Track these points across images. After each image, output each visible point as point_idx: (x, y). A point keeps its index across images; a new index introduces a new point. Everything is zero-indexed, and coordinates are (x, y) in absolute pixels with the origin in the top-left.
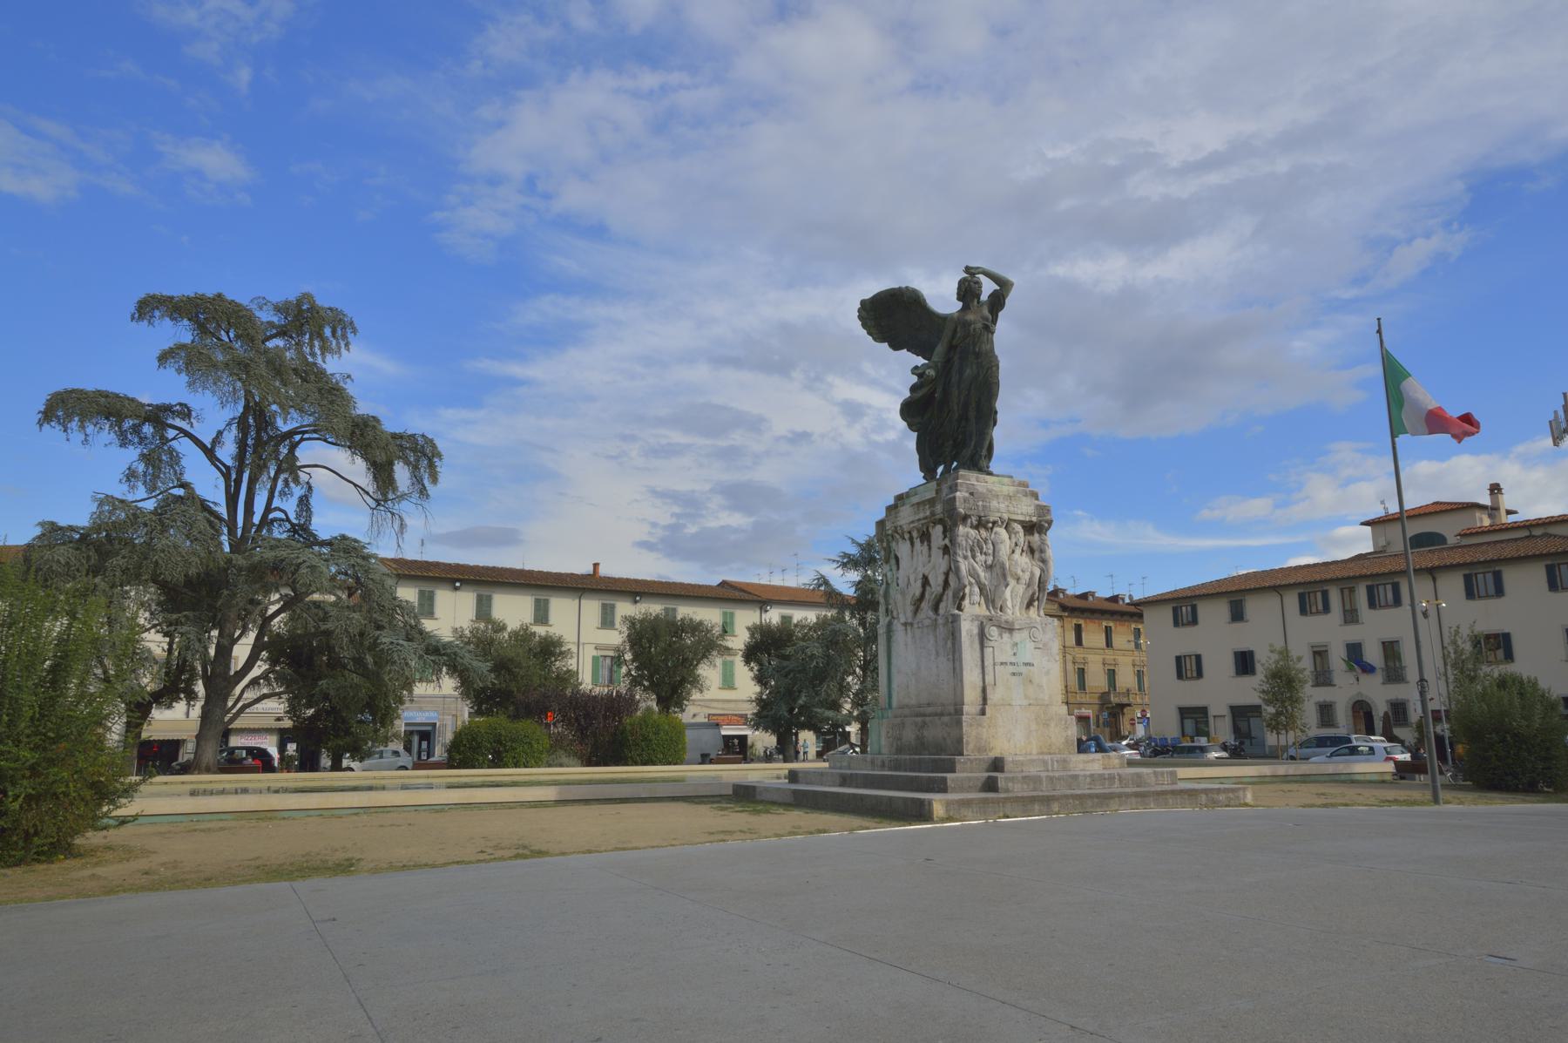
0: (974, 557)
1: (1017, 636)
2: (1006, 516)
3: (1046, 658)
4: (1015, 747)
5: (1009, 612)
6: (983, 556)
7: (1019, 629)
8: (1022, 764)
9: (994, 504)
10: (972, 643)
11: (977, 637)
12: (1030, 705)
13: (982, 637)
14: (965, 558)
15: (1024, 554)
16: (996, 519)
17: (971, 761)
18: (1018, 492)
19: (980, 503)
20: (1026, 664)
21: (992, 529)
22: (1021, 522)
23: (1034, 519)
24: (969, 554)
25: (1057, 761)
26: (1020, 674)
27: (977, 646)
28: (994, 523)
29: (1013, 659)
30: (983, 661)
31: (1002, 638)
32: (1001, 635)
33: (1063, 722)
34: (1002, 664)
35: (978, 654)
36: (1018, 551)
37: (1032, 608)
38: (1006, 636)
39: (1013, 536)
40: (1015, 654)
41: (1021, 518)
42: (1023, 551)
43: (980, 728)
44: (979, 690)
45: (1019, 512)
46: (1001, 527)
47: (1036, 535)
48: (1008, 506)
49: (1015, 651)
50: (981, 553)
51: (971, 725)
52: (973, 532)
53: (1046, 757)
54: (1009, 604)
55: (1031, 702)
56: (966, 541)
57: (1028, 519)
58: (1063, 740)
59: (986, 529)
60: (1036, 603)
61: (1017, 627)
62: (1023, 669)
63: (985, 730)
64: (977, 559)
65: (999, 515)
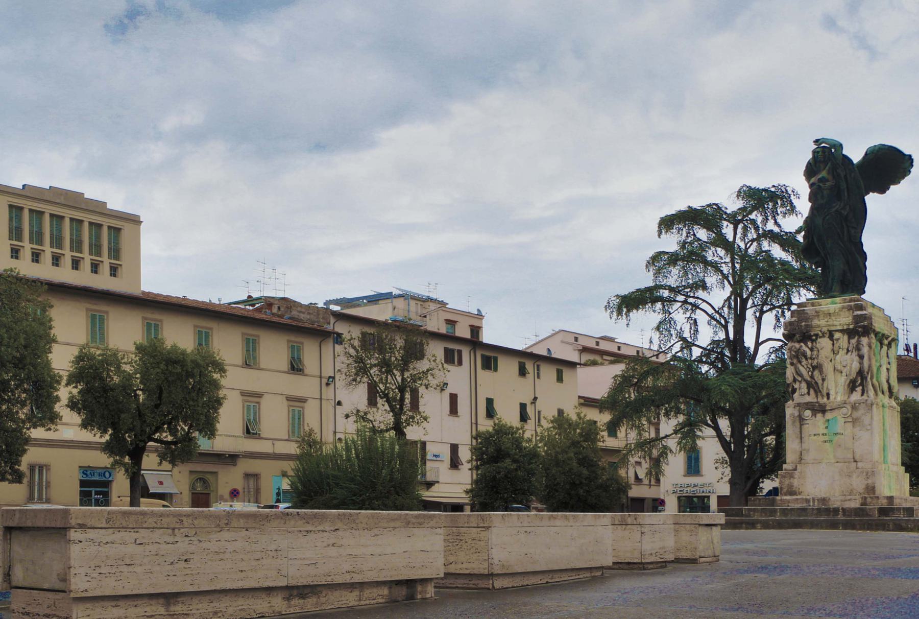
0: (800, 362)
1: (829, 415)
2: (825, 329)
3: (858, 428)
4: (821, 491)
5: (832, 397)
6: (810, 361)
7: (831, 410)
8: (789, 502)
9: (816, 322)
10: (794, 422)
11: (798, 419)
12: (837, 462)
13: (801, 420)
14: (792, 364)
15: (850, 353)
16: (816, 332)
17: (760, 500)
18: (843, 308)
19: (803, 324)
20: (836, 434)
21: (817, 339)
22: (842, 331)
23: (851, 327)
24: (795, 361)
25: (818, 500)
27: (798, 424)
28: (817, 335)
29: (825, 431)
30: (801, 434)
31: (816, 417)
32: (814, 415)
33: (865, 474)
34: (815, 435)
35: (798, 430)
36: (842, 353)
37: (854, 392)
38: (819, 415)
39: (835, 342)
40: (826, 428)
41: (839, 328)
42: (848, 351)
43: (792, 479)
44: (799, 453)
45: (838, 323)
46: (823, 336)
47: (856, 338)
48: (828, 321)
49: (826, 425)
50: (806, 359)
51: (785, 477)
52: (797, 345)
53: (808, 497)
54: (832, 393)
55: (839, 460)
56: (790, 352)
57: (845, 327)
58: (864, 486)
59: (813, 341)
60: (859, 389)
61: (828, 408)
62: (836, 438)
63: (795, 480)
64: (803, 364)
65: (819, 329)
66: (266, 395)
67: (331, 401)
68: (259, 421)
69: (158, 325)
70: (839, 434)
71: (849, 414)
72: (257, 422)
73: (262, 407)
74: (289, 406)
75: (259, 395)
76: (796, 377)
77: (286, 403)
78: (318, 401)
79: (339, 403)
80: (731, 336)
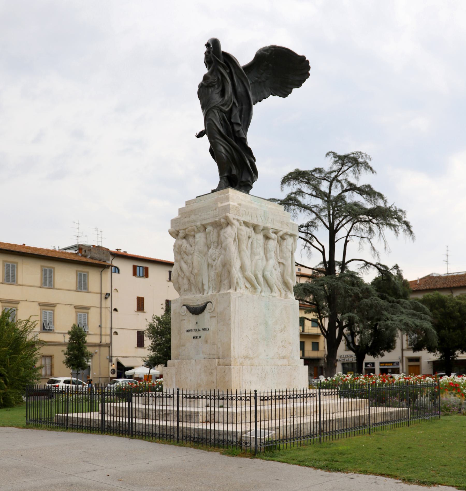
26: (200, 337)
29: (196, 328)
55: (205, 356)
66: (58, 306)
67: (109, 309)
68: (88, 324)
69: (86, 274)
70: (205, 329)
71: (213, 309)
72: (52, 322)
73: (56, 313)
74: (76, 312)
75: (54, 305)
76: (180, 273)
77: (74, 310)
78: (99, 309)
79: (116, 310)
80: (327, 259)
